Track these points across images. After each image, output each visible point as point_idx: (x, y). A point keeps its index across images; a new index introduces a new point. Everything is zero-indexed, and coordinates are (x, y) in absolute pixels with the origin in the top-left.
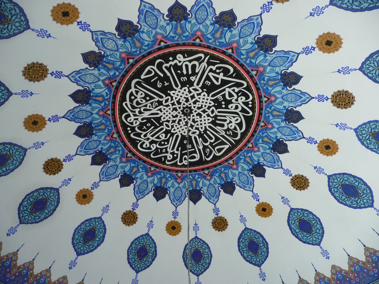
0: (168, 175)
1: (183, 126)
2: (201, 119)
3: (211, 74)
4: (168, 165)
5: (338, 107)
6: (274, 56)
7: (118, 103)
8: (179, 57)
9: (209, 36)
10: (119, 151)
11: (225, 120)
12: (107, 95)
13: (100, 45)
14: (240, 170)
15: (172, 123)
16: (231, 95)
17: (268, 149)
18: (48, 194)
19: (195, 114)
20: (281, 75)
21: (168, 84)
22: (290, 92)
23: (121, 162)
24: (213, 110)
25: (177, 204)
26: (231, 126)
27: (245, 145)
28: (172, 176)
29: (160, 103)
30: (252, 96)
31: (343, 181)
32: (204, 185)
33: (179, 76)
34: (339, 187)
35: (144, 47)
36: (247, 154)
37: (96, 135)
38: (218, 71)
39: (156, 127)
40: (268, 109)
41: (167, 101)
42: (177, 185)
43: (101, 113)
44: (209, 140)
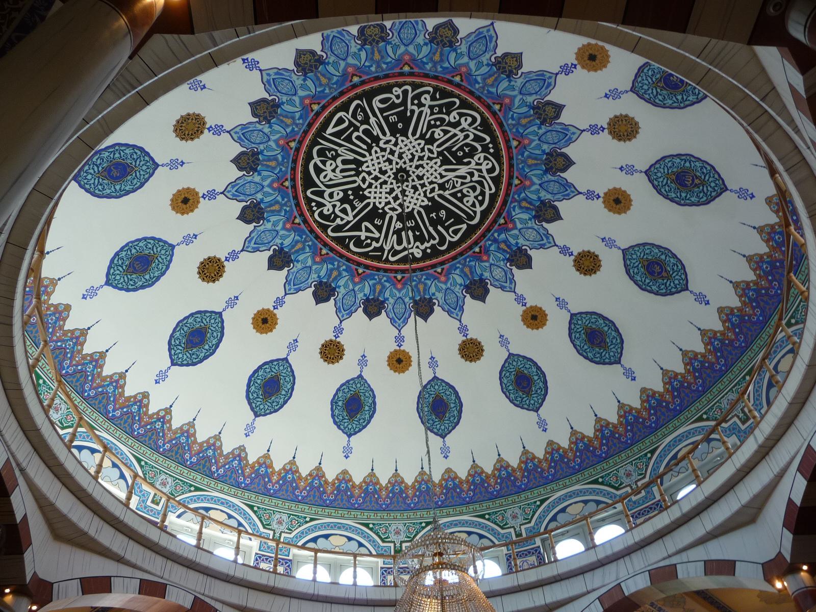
0: (428, 67)
1: (407, 151)
2: (380, 166)
3: (377, 235)
4: (429, 85)
5: (209, 258)
6: (310, 281)
9: (387, 284)
10: (512, 118)
11: (342, 171)
13: (509, 275)
14: (296, 99)
15: (424, 156)
16: (344, 211)
18: (650, 91)
19: (390, 173)
20: (292, 260)
22: (271, 244)
23: (512, 98)
24: (364, 183)
26: (331, 164)
27: (300, 142)
29: (442, 187)
31: (136, 176)
32: (356, 56)
33: (416, 228)
34: (134, 163)
36: (293, 129)
37: (543, 151)
38: (369, 241)
39: (448, 149)
40: (288, 209)
41: (433, 190)
42: (411, 49)
43: (527, 183)
44: (361, 134)
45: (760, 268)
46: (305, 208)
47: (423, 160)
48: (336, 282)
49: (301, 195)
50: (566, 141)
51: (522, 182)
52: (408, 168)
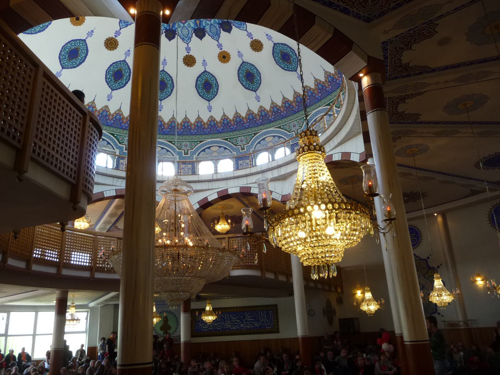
45: (236, 118)
50: (238, 26)
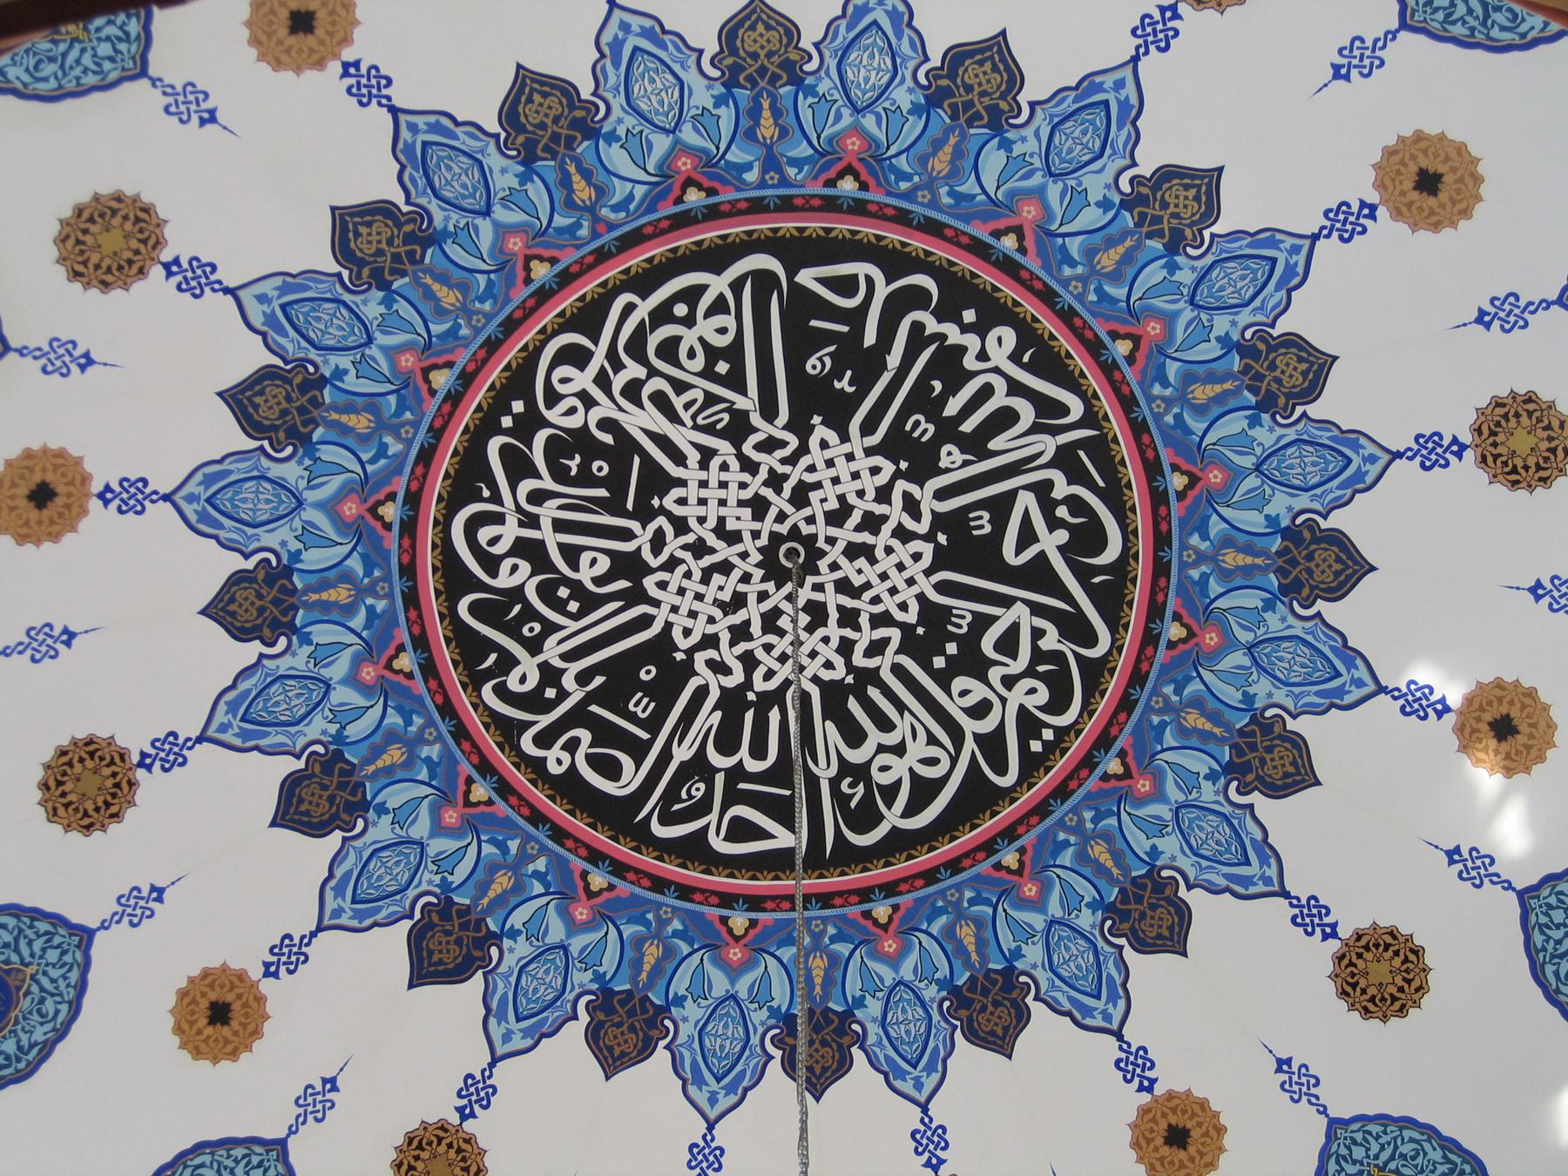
1: (709, 599)
5: (1344, 994)
6: (1298, 628)
7: (612, 272)
8: (1000, 340)
9: (1172, 369)
10: (382, 451)
11: (885, 725)
12: (622, 206)
13: (844, 35)
15: (685, 547)
16: (1008, 644)
17: (938, 982)
20: (1253, 720)
21: (850, 390)
22: (1227, 809)
23: (330, 507)
24: (885, 642)
25: (337, 913)
27: (865, 894)
28: (441, 772)
29: (738, 429)
30: (1081, 715)
33: (922, 400)
35: (944, 190)
36: (833, 939)
37: (387, 302)
38: (1062, 512)
39: (614, 505)
40: (1088, 815)
41: (769, 445)
46: (1061, 764)
47: (701, 540)
48: (1260, 542)
49: (1026, 798)
51: (528, 259)
52: (756, 557)
